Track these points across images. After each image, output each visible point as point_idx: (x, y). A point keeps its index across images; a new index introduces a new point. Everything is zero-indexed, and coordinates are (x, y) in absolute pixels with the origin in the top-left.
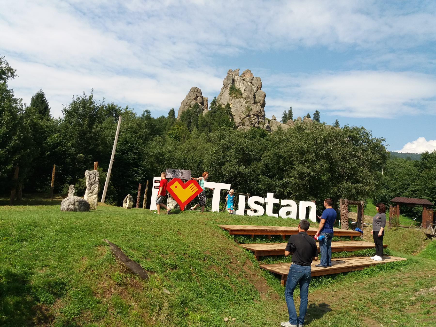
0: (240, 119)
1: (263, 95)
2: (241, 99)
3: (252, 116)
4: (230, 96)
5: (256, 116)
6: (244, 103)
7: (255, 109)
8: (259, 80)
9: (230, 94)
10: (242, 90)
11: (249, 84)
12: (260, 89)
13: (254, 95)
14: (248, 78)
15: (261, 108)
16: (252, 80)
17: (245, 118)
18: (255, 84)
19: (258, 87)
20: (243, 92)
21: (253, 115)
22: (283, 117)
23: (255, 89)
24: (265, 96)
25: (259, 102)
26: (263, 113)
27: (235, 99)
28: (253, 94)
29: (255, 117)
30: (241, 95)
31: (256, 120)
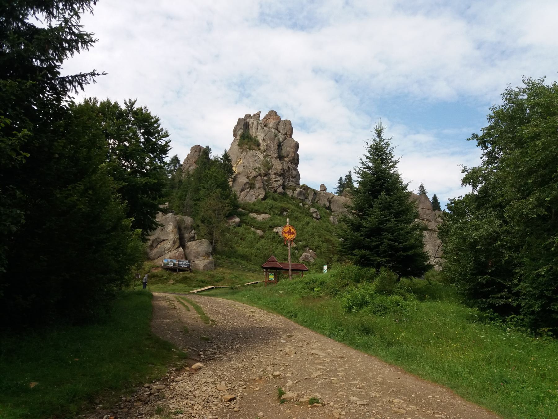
0: (248, 178)
1: (293, 144)
2: (258, 152)
3: (272, 176)
4: (238, 147)
5: (280, 176)
6: (262, 157)
7: (278, 165)
8: (288, 123)
9: (239, 145)
10: (260, 139)
11: (273, 130)
12: (291, 137)
13: (279, 146)
14: (271, 123)
15: (290, 165)
16: (278, 124)
17: (256, 177)
18: (281, 130)
19: (286, 134)
20: (261, 141)
21: (275, 174)
22: (339, 187)
23: (281, 137)
24: (297, 146)
25: (288, 155)
26: (294, 172)
27: (247, 152)
28: (276, 142)
29: (279, 178)
30: (259, 145)
31: (281, 182)
